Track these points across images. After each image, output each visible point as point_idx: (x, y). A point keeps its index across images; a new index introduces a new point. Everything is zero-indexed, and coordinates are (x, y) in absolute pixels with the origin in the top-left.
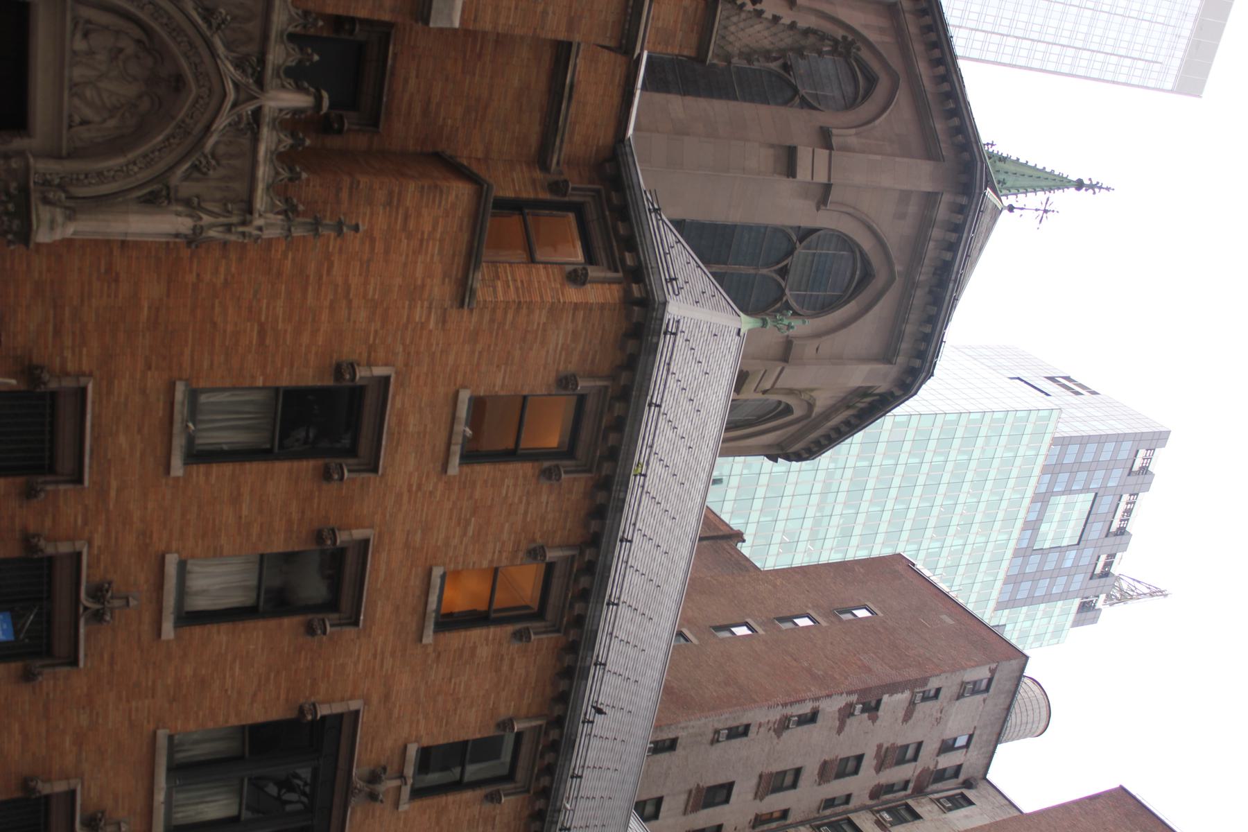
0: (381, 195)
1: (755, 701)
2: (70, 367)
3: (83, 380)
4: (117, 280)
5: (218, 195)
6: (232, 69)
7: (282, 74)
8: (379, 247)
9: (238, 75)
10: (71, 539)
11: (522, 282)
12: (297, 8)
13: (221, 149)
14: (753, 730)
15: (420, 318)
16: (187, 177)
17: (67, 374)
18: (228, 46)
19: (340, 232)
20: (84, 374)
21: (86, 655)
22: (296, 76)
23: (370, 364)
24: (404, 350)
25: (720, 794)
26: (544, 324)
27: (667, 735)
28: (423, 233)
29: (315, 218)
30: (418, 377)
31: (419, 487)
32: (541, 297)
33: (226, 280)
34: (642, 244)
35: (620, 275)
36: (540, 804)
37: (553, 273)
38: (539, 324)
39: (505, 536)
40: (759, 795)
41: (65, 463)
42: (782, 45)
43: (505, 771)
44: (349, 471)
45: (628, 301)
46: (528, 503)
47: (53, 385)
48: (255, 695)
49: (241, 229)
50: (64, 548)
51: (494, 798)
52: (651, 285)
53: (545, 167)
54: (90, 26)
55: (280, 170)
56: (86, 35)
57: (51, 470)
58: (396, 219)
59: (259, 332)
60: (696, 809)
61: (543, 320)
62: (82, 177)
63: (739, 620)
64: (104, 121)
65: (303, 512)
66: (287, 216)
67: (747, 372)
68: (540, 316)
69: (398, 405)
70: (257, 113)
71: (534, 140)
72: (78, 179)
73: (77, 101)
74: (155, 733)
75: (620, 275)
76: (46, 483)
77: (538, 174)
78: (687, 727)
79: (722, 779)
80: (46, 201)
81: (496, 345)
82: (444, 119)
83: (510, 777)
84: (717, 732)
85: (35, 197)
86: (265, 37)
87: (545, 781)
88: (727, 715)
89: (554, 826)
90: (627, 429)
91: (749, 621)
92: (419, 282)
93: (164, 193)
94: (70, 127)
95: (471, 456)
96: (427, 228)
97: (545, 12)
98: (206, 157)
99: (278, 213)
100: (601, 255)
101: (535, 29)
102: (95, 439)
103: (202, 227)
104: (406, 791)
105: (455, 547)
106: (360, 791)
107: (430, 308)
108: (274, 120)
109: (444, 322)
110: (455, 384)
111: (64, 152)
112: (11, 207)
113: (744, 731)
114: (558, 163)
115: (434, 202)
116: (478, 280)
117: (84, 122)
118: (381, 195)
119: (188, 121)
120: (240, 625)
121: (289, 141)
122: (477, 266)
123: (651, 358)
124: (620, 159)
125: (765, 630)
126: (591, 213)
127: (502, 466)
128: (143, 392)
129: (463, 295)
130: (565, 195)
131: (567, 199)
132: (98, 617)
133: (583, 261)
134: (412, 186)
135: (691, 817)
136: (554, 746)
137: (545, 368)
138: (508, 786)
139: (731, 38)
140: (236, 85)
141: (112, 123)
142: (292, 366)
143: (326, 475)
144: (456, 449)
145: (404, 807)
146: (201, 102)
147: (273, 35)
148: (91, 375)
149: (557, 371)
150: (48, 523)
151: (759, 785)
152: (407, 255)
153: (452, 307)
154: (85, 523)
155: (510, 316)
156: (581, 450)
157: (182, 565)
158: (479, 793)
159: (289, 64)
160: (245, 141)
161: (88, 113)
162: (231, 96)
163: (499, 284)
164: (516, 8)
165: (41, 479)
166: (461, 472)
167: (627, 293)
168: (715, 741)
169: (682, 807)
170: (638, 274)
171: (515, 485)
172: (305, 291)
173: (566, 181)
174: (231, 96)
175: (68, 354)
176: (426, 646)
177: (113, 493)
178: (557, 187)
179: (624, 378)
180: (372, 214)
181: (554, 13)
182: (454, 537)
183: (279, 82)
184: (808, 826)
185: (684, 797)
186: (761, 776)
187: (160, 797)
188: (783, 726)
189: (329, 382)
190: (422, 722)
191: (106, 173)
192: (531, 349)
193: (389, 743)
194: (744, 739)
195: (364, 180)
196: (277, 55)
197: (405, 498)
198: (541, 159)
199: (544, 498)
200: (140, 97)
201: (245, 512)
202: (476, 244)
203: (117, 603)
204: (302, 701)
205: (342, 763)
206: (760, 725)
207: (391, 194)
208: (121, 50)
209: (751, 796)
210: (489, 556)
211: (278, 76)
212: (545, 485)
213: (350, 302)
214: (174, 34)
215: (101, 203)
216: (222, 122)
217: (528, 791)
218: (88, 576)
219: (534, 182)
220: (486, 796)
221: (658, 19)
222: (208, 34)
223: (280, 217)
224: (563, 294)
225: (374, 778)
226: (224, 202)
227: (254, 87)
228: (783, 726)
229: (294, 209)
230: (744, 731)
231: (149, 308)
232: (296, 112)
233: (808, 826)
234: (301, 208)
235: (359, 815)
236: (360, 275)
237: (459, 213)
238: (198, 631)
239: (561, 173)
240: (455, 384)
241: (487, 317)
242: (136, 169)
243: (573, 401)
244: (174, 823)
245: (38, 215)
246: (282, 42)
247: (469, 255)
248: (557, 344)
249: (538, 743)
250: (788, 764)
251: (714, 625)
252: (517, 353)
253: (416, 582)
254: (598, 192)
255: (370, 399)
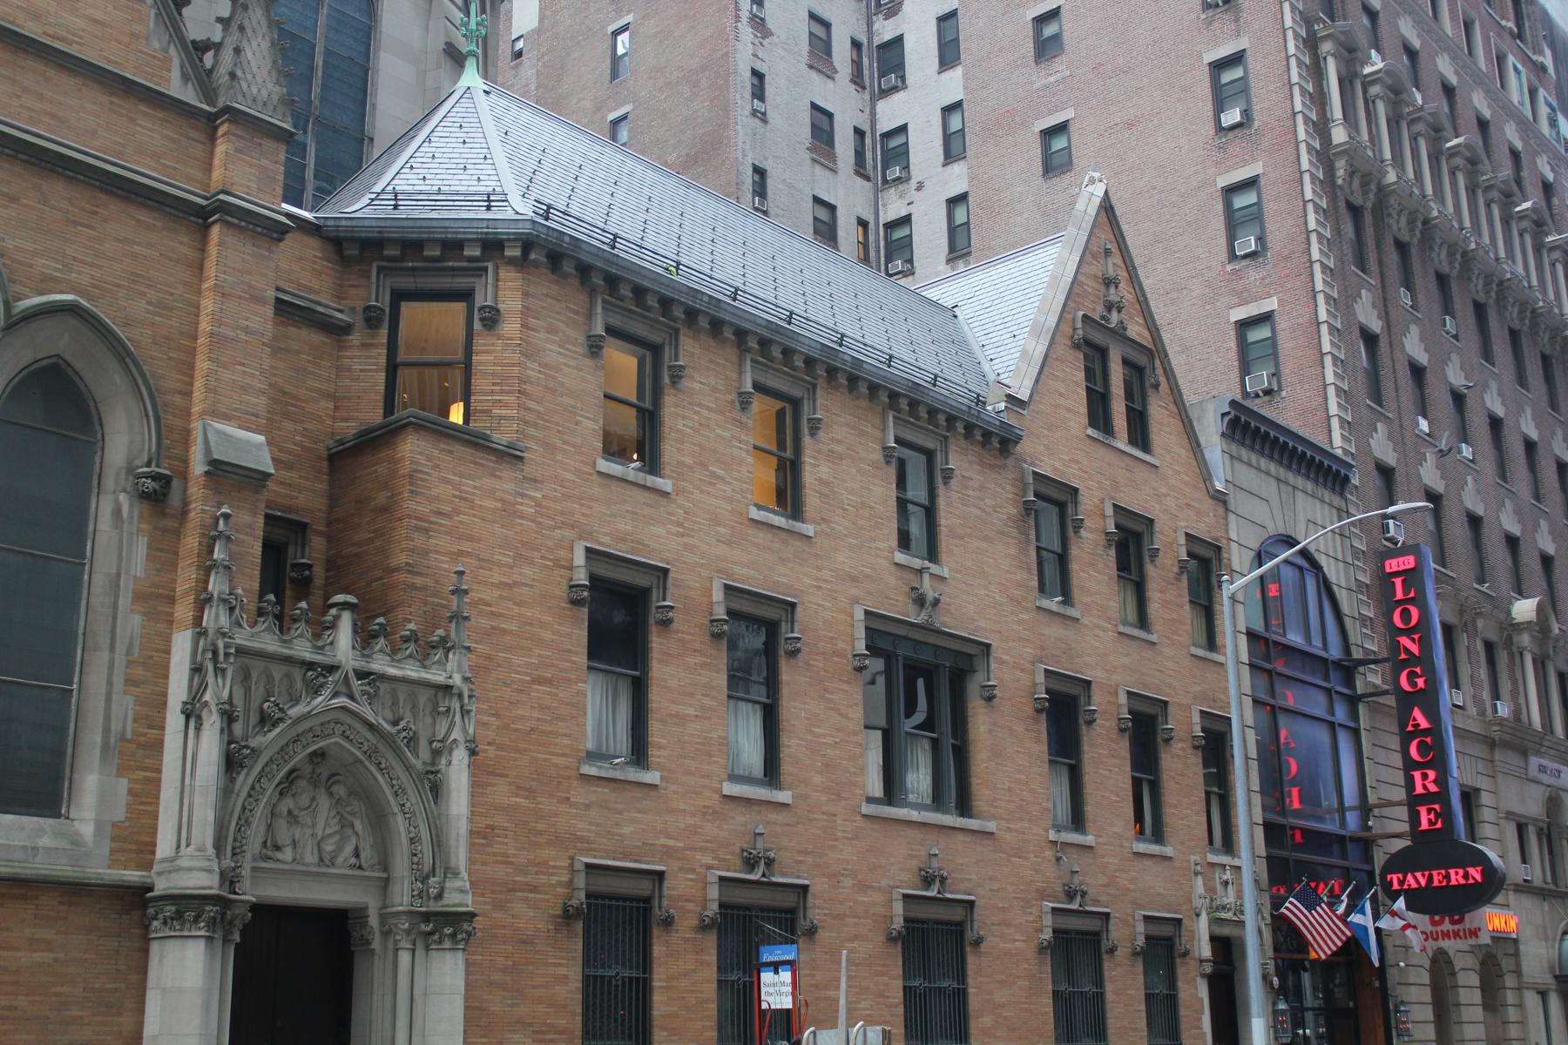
0: (419, 540)
1: (727, 54)
2: (565, 879)
3: (578, 866)
4: (493, 828)
5: (429, 720)
6: (320, 699)
7: (320, 643)
8: (466, 546)
9: (326, 693)
10: (705, 885)
11: (494, 384)
12: (256, 622)
13: (390, 716)
14: (759, 67)
15: (531, 507)
16: (417, 756)
17: (571, 881)
18: (296, 701)
19: (466, 592)
20: (572, 865)
21: (798, 877)
22: (322, 629)
23: (571, 568)
24: (560, 528)
25: (822, 123)
26: (540, 365)
27: (748, 177)
28: (455, 496)
29: (451, 619)
30: (584, 515)
31: (680, 524)
32: (513, 365)
33: (494, 715)
34: (456, 233)
35: (490, 265)
36: (960, 427)
37: (485, 345)
38: (540, 372)
39: (727, 434)
40: (830, 74)
41: (643, 887)
42: (264, 22)
43: (922, 459)
44: (664, 600)
45: (522, 263)
46: (700, 405)
47: (582, 895)
48: (841, 715)
49: (466, 700)
50: (714, 893)
51: (948, 475)
52: (508, 234)
53: (345, 330)
54: (269, 843)
55: (408, 652)
56: (278, 848)
57: (647, 900)
58: (441, 525)
59: (540, 684)
60: (832, 157)
61: (535, 366)
62: (415, 859)
63: (609, 42)
64: (357, 834)
65: (695, 651)
66: (449, 649)
67: (446, 43)
68: (533, 370)
69: (607, 539)
70: (362, 675)
71: (317, 338)
72: (418, 864)
73: (340, 860)
74: (864, 816)
75: (490, 265)
76: (660, 908)
77: (355, 338)
78: (743, 150)
79: (805, 117)
80: (439, 896)
81: (557, 424)
82: (295, 444)
83: (929, 455)
84: (754, 113)
85: (433, 907)
86: (288, 660)
87: (941, 418)
88: (738, 96)
89: (982, 416)
90: (646, 284)
91: (611, 29)
92: (499, 505)
93: (431, 777)
94: (360, 867)
95: (652, 463)
96: (449, 490)
97: (246, 330)
98: (399, 732)
99: (447, 657)
100: (462, 282)
101: (264, 344)
102: (625, 857)
103: (467, 741)
104: (934, 568)
105: (733, 491)
106: (930, 616)
107: (523, 495)
108: (363, 656)
109: (535, 481)
110: (591, 474)
111: (384, 875)
112: (448, 931)
113: (758, 75)
114: (341, 311)
115: (423, 480)
116: (501, 438)
117: (357, 854)
118: (419, 540)
119: (365, 748)
120: (784, 725)
121: (382, 641)
122: (487, 438)
123: (584, 246)
124: (342, 235)
125: (629, 12)
126: (407, 283)
127: (666, 430)
128: (588, 806)
129: (511, 456)
130: (383, 311)
131: (387, 310)
132: (770, 863)
133: (464, 304)
134: (410, 505)
135: (840, 164)
136: (914, 404)
137: (580, 370)
138: (939, 458)
139: (264, 93)
140: (335, 695)
141: (358, 826)
142: (569, 651)
143: (666, 623)
144: (651, 480)
145: (946, 573)
146: (348, 733)
147: (286, 651)
148: (572, 858)
149: (584, 355)
150: (691, 906)
151: (819, 71)
152: (474, 516)
153: (522, 470)
154: (693, 871)
155: (532, 405)
156: (656, 338)
157: (734, 778)
158: (941, 490)
159: (310, 637)
160: (384, 687)
161: (349, 848)
162: (342, 701)
163: (496, 411)
164: (243, 365)
165: (656, 910)
166: (670, 477)
167: (512, 262)
168: (763, 117)
169: (827, 173)
170: (493, 245)
171: (684, 418)
172: (505, 632)
173: (367, 309)
174: (342, 701)
175: (554, 879)
176: (816, 533)
177: (671, 842)
178: (372, 319)
179: (598, 280)
180: (437, 552)
181: (247, 319)
182: (725, 491)
183: (327, 648)
184: (874, 18)
185: (818, 169)
186: (811, 67)
187: (914, 815)
188: (759, 24)
189: (584, 612)
190: (879, 544)
191: (412, 835)
192: (563, 383)
193: (892, 581)
194: (767, 78)
195: (401, 559)
196: (302, 649)
197: (686, 540)
198: (338, 331)
199: (697, 386)
200: (331, 794)
201: (691, 711)
202: (467, 437)
203: (760, 845)
204: (850, 668)
205: (902, 631)
206: (755, 55)
207: (418, 529)
208: (290, 812)
209: (830, 84)
210: (744, 454)
211: (322, 648)
212: (685, 383)
213: (515, 583)
214: (287, 757)
215: (439, 842)
216: (367, 712)
217: (946, 438)
218: (735, 871)
219: (364, 346)
220: (945, 484)
221: (248, 187)
222: (289, 722)
223: (451, 656)
224: (510, 339)
225: (920, 601)
226: (435, 713)
227: (337, 676)
228: (759, 24)
229: (444, 640)
230: (758, 75)
231: (517, 796)
232: (355, 632)
233: (874, 18)
234: (441, 632)
235: (947, 619)
236: (491, 570)
237: (436, 452)
238: (786, 767)
239: (353, 310)
240: (591, 474)
241: (532, 431)
242: (408, 805)
243: (611, 340)
244: (929, 801)
245: (454, 906)
246: (290, 641)
247: (475, 445)
248: (560, 353)
249: (905, 421)
250: (803, 27)
251: (609, 77)
252: (566, 400)
253: (762, 537)
254: (380, 269)
255: (605, 571)
